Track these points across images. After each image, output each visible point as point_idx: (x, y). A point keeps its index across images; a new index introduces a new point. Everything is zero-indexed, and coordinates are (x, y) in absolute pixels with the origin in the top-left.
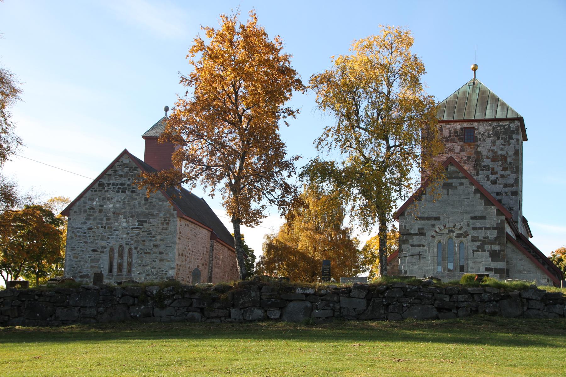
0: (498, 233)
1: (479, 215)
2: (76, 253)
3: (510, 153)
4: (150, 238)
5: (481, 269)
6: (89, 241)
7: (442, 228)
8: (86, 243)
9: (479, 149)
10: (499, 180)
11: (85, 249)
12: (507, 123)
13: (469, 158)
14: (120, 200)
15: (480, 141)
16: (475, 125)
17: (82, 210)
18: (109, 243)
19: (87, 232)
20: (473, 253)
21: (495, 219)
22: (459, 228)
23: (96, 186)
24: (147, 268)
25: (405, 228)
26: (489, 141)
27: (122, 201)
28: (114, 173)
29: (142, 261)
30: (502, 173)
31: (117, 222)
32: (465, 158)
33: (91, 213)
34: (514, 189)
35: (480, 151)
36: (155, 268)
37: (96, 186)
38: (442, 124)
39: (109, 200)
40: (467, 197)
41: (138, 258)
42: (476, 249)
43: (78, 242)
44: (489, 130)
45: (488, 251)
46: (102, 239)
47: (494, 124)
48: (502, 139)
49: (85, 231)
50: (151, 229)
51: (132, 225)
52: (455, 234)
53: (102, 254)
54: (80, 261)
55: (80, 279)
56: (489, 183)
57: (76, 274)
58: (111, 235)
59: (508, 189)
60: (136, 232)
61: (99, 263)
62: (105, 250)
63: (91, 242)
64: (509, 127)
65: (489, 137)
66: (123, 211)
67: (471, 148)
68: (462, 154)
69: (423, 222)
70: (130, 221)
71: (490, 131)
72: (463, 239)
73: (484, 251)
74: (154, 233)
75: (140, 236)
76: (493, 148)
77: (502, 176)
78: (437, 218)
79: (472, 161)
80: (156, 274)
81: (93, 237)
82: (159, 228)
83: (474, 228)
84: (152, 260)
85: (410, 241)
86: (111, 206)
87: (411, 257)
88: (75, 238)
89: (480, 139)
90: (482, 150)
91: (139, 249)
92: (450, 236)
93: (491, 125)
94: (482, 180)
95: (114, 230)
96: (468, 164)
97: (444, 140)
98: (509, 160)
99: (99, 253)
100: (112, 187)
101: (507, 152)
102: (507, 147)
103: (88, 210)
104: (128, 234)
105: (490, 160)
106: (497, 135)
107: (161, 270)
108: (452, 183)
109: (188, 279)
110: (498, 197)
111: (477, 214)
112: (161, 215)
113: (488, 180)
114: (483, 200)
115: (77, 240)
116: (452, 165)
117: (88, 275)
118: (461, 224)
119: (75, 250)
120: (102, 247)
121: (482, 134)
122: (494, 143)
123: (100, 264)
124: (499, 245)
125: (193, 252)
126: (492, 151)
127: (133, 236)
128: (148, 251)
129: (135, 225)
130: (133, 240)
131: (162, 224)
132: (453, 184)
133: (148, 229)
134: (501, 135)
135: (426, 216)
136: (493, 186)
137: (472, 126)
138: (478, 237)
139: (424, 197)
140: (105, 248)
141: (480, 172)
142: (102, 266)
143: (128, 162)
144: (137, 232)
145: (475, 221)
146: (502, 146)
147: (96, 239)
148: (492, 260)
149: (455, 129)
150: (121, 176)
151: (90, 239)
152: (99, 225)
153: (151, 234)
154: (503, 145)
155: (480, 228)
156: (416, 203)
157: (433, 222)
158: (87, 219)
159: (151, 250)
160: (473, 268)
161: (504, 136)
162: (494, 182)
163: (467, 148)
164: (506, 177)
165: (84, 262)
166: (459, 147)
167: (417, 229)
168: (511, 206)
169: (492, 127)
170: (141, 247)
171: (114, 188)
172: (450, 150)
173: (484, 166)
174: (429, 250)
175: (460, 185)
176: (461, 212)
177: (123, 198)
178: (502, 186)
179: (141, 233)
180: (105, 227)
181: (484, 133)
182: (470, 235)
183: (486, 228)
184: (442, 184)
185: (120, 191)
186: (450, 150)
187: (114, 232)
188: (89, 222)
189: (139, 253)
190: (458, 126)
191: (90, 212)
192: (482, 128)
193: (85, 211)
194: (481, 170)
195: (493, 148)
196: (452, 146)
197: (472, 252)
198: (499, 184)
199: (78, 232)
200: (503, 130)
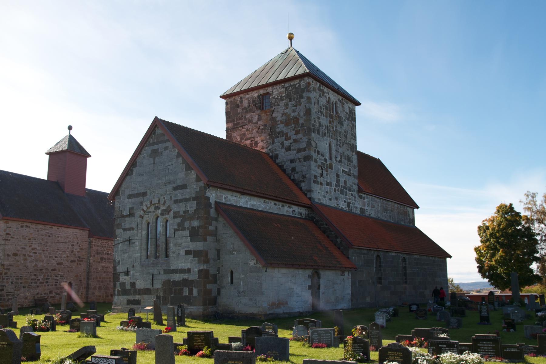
0: (197, 204)
1: (181, 184)
3: (302, 114)
5: (181, 253)
7: (149, 205)
9: (274, 115)
10: (292, 146)
12: (298, 81)
13: (265, 126)
15: (275, 106)
16: (270, 89)
20: (174, 233)
21: (195, 187)
22: (162, 203)
25: (119, 210)
26: (282, 104)
30: (294, 137)
32: (262, 127)
34: (306, 153)
35: (275, 117)
38: (242, 95)
40: (170, 163)
42: (176, 227)
44: (282, 93)
45: (188, 229)
47: (287, 85)
48: (293, 101)
52: (160, 211)
56: (284, 150)
59: (301, 155)
64: (300, 85)
65: (282, 100)
67: (267, 116)
68: (260, 123)
69: (133, 200)
71: (283, 93)
72: (167, 216)
73: (184, 229)
76: (286, 111)
77: (295, 141)
78: (144, 194)
79: (268, 129)
83: (176, 202)
85: (123, 224)
87: (123, 243)
89: (274, 104)
90: (277, 115)
92: (156, 215)
93: (283, 87)
94: (277, 148)
96: (265, 132)
97: (244, 111)
98: (301, 121)
101: (298, 113)
102: (298, 107)
105: (283, 125)
106: (289, 97)
108: (158, 149)
109: (33, 277)
110: (293, 165)
111: (179, 183)
113: (283, 147)
114: (184, 165)
116: (158, 128)
118: (164, 198)
121: (276, 98)
122: (286, 105)
124: (198, 219)
125: (43, 251)
126: (286, 114)
132: (159, 151)
134: (293, 96)
135: (136, 192)
136: (287, 153)
137: (267, 91)
138: (179, 212)
139: (135, 169)
141: (276, 140)
145: (176, 192)
146: (294, 108)
148: (191, 241)
149: (253, 98)
154: (296, 106)
155: (181, 201)
156: (128, 178)
157: (140, 199)
160: (174, 253)
161: (295, 96)
162: (288, 149)
163: (264, 116)
164: (299, 141)
166: (257, 117)
167: (128, 209)
168: (304, 173)
169: (284, 89)
172: (250, 121)
173: (279, 133)
174: (137, 234)
175: (165, 150)
176: (165, 183)
178: (295, 152)
181: (278, 96)
182: (172, 211)
183: (187, 200)
184: (150, 152)
186: (250, 121)
190: (255, 94)
192: (276, 92)
194: (276, 138)
195: (286, 111)
196: (251, 116)
197: (173, 231)
198: (293, 150)
200: (294, 90)
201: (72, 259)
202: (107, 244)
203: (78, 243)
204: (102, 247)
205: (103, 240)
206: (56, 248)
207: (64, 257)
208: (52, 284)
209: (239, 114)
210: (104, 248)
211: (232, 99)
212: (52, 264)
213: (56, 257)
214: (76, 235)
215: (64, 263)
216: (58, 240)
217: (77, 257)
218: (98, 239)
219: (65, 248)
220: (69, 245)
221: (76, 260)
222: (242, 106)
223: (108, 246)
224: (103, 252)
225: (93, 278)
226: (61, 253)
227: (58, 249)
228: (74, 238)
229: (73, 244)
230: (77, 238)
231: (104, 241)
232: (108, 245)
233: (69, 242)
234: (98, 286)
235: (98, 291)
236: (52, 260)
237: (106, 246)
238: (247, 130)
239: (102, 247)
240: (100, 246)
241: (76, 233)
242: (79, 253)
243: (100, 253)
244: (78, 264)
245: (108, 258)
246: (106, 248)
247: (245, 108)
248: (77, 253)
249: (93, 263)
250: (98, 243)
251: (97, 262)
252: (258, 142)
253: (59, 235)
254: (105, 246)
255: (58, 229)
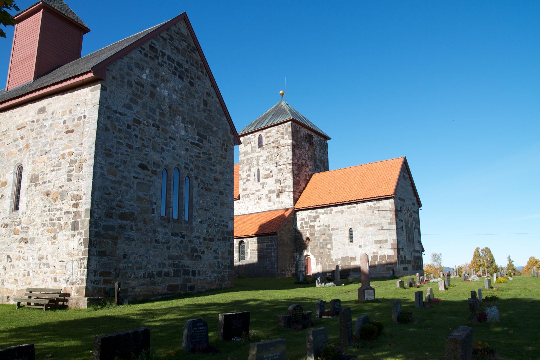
2: (113, 164)
4: (211, 167)
6: (136, 145)
8: (130, 147)
9: (316, 153)
11: (129, 159)
13: (312, 156)
14: (177, 89)
16: (313, 134)
17: (126, 81)
18: (164, 158)
19: (132, 127)
23: (146, 46)
24: (209, 214)
27: (179, 92)
28: (170, 40)
29: (203, 202)
31: (174, 125)
33: (139, 93)
36: (216, 216)
37: (146, 46)
38: (300, 126)
39: (163, 80)
41: (199, 195)
43: (118, 142)
46: (154, 149)
49: (130, 123)
50: (211, 153)
51: (191, 138)
52: (408, 214)
53: (155, 177)
54: (120, 183)
55: (119, 221)
57: (112, 209)
58: (166, 145)
60: (196, 150)
61: (151, 193)
62: (158, 170)
63: (138, 149)
66: (181, 109)
68: (309, 152)
70: (189, 130)
74: (213, 160)
75: (200, 159)
80: (218, 226)
81: (141, 138)
82: (218, 153)
84: (213, 202)
86: (166, 93)
88: (111, 131)
91: (199, 180)
95: (171, 138)
99: (149, 173)
100: (167, 62)
103: (134, 85)
104: (187, 150)
106: (321, 145)
107: (222, 219)
112: (220, 134)
115: (116, 137)
117: (134, 214)
119: (112, 156)
120: (154, 163)
122: (320, 150)
123: (151, 196)
127: (192, 156)
128: (209, 186)
129: (195, 139)
130: (192, 163)
131: (221, 148)
133: (209, 150)
134: (323, 147)
140: (159, 166)
142: (154, 200)
143: (186, 34)
144: (197, 151)
147: (146, 144)
149: (305, 133)
150: (178, 50)
151: (136, 142)
152: (150, 121)
153: (210, 159)
158: (132, 100)
159: (211, 185)
165: (126, 185)
170: (202, 178)
171: (169, 64)
177: (180, 87)
179: (201, 155)
180: (158, 127)
185: (177, 74)
187: (169, 140)
188: (136, 108)
189: (200, 188)
190: (307, 131)
191: (137, 89)
192: (316, 138)
193: (130, 85)
199: (118, 120)
209: (299, 138)
211: (294, 124)
222: (300, 134)
238: (303, 153)
247: (301, 136)
252: (309, 165)
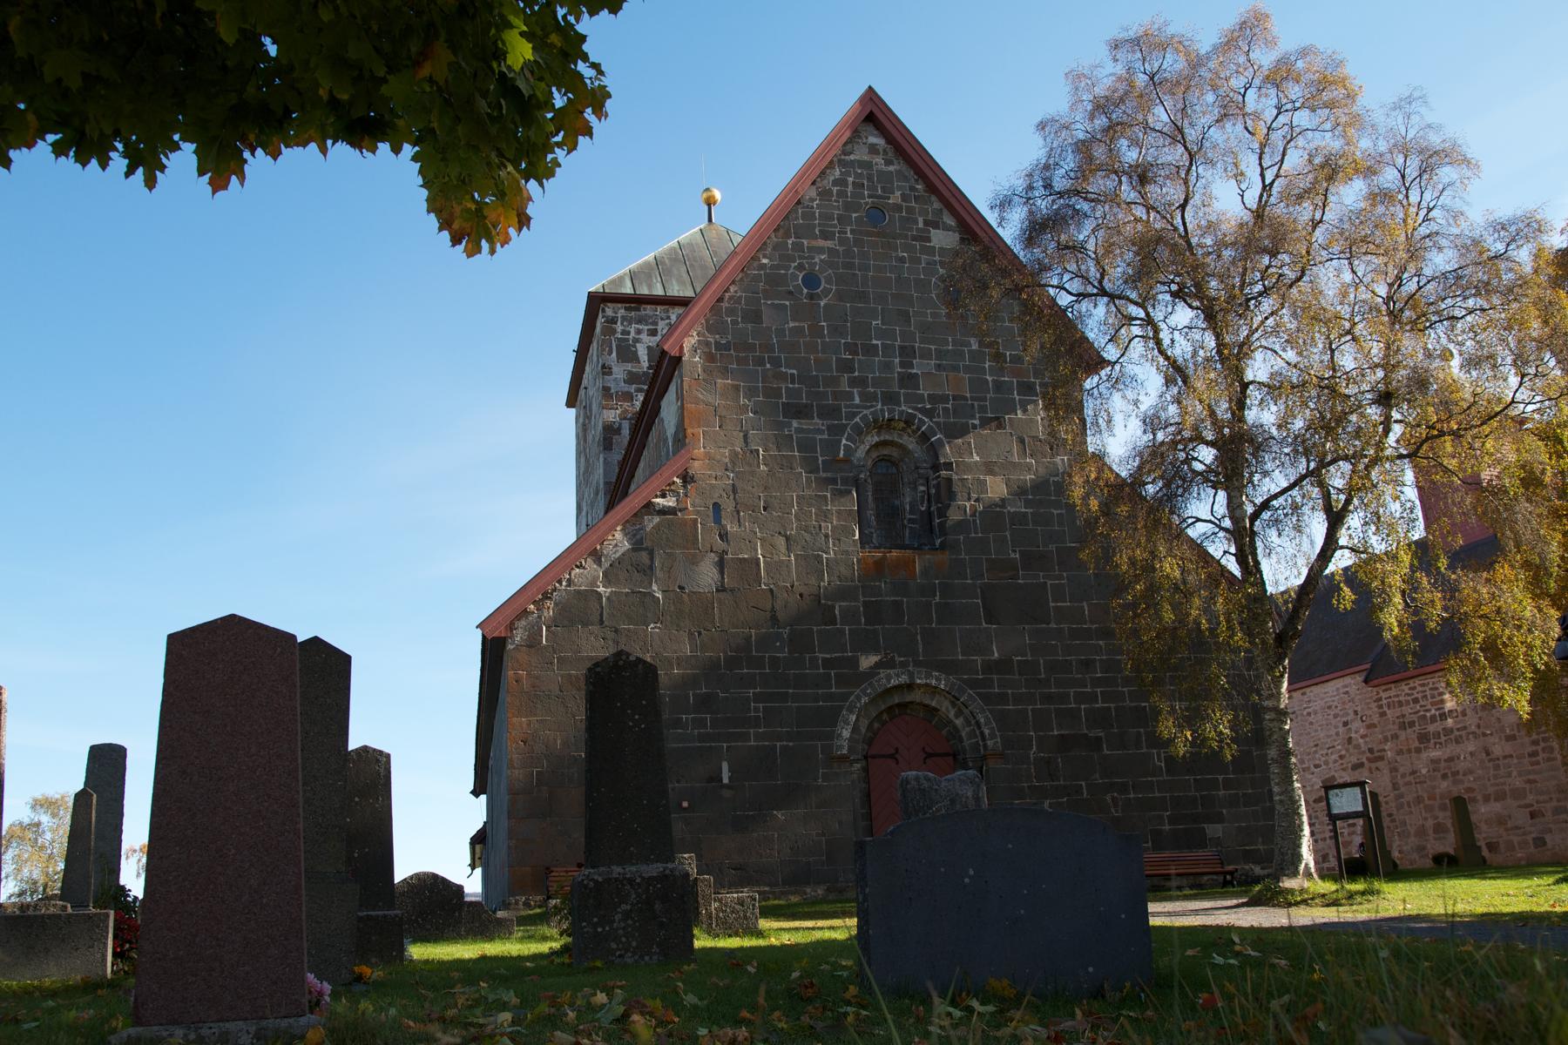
201: (1354, 760)
202: (1427, 688)
203: (1356, 713)
204: (1416, 701)
205: (1411, 681)
206: (1312, 744)
207: (1335, 761)
208: (1322, 836)
210: (1423, 703)
212: (1313, 786)
213: (1316, 766)
214: (1347, 693)
215: (1336, 775)
216: (1311, 723)
217: (1364, 752)
218: (1394, 682)
219: (1328, 736)
220: (1336, 727)
221: (1364, 760)
223: (1436, 692)
224: (1425, 716)
225: (1409, 803)
226: (1325, 752)
227: (1316, 745)
228: (1344, 703)
229: (1345, 719)
230: (1352, 700)
231: (1417, 682)
232: (1431, 689)
233: (1336, 716)
234: (1430, 823)
235: (1435, 839)
236: (1311, 776)
237: (1428, 693)
239: (1416, 701)
240: (1408, 702)
241: (1346, 686)
242: (1367, 739)
243: (1412, 724)
244: (1370, 769)
245: (1444, 729)
246: (1430, 700)
248: (1361, 741)
249: (1398, 758)
250: (1398, 696)
251: (1409, 751)
253: (1310, 710)
254: (1425, 696)
255: (1303, 694)
